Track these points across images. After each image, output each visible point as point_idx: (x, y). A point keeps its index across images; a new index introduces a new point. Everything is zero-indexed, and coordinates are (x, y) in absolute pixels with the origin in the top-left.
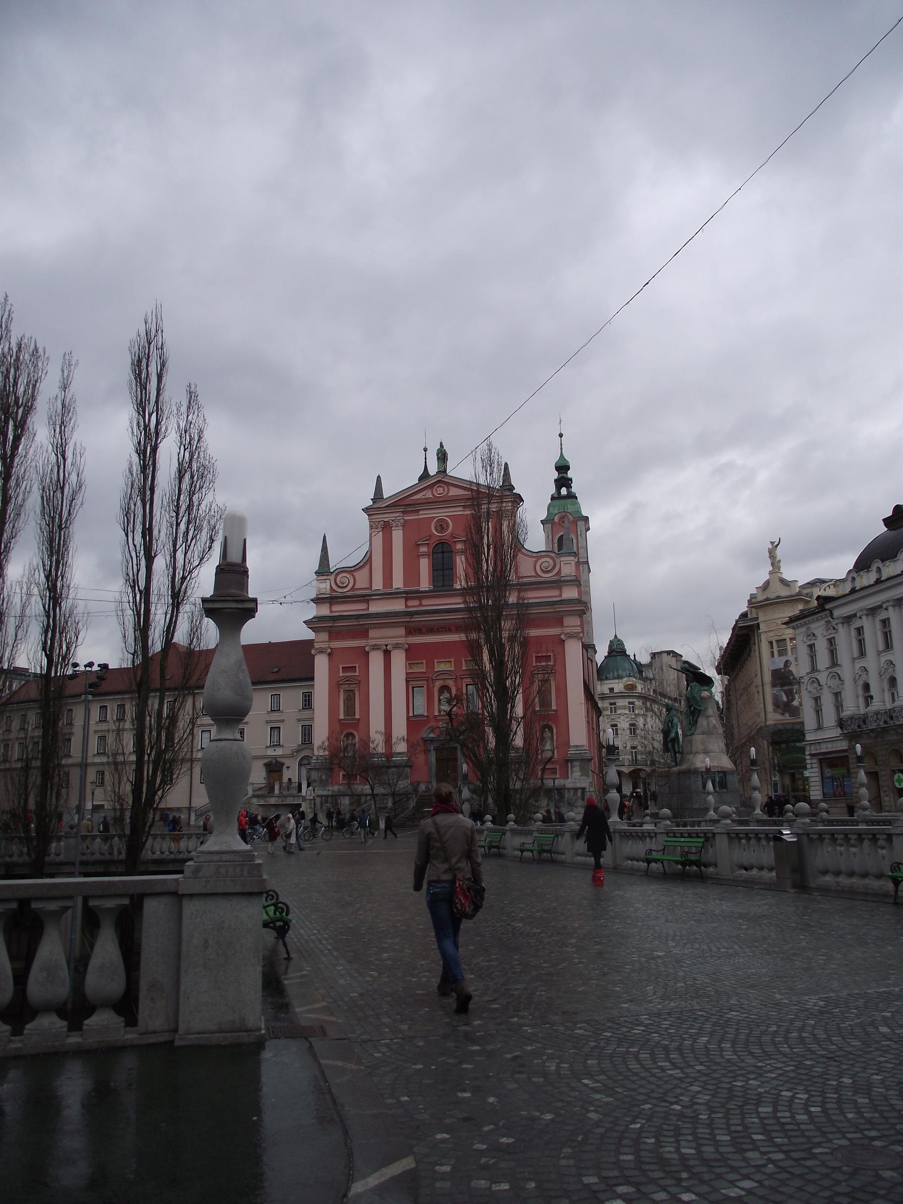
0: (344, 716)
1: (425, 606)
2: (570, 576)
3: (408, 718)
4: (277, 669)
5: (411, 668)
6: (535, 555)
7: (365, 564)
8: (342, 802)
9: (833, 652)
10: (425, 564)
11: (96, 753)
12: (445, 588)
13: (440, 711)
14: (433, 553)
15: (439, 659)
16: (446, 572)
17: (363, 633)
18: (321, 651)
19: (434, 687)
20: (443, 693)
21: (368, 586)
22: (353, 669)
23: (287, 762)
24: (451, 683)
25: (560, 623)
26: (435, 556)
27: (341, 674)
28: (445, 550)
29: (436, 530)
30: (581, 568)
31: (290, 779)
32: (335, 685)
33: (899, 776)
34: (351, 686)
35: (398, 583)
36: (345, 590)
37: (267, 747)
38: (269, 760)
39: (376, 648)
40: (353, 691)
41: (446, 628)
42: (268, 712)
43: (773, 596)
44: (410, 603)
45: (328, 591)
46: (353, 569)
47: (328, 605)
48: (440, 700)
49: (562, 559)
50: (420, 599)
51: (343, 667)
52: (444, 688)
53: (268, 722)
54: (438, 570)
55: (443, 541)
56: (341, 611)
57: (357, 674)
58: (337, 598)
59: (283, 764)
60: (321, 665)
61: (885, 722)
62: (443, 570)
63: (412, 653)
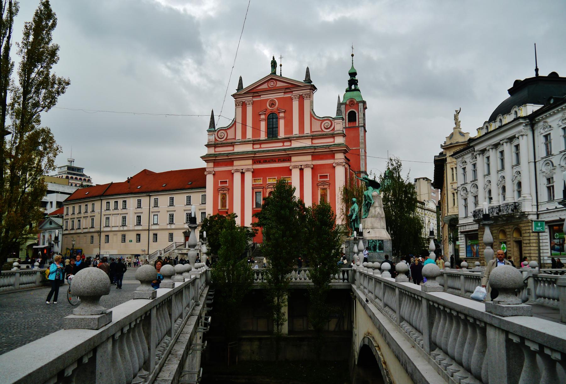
2: (339, 130)
3: (253, 208)
4: (191, 183)
5: (255, 182)
7: (233, 125)
9: (475, 171)
10: (263, 125)
11: (121, 225)
12: (273, 139)
14: (268, 119)
15: (270, 177)
16: (274, 129)
17: (230, 162)
18: (210, 173)
21: (234, 138)
22: (226, 182)
25: (333, 157)
26: (269, 120)
27: (220, 185)
28: (274, 117)
29: (270, 106)
30: (360, 130)
32: (217, 190)
33: (504, 246)
34: (225, 191)
35: (249, 135)
36: (222, 140)
37: (184, 224)
38: (186, 230)
39: (237, 171)
40: (225, 194)
41: (273, 160)
42: (185, 205)
43: (455, 142)
44: (255, 146)
45: (214, 141)
46: (226, 128)
47: (213, 148)
49: (336, 121)
50: (260, 144)
53: (185, 210)
54: (270, 128)
55: (273, 112)
57: (228, 185)
58: (218, 144)
60: (210, 179)
61: (497, 213)
62: (273, 128)
63: (256, 173)
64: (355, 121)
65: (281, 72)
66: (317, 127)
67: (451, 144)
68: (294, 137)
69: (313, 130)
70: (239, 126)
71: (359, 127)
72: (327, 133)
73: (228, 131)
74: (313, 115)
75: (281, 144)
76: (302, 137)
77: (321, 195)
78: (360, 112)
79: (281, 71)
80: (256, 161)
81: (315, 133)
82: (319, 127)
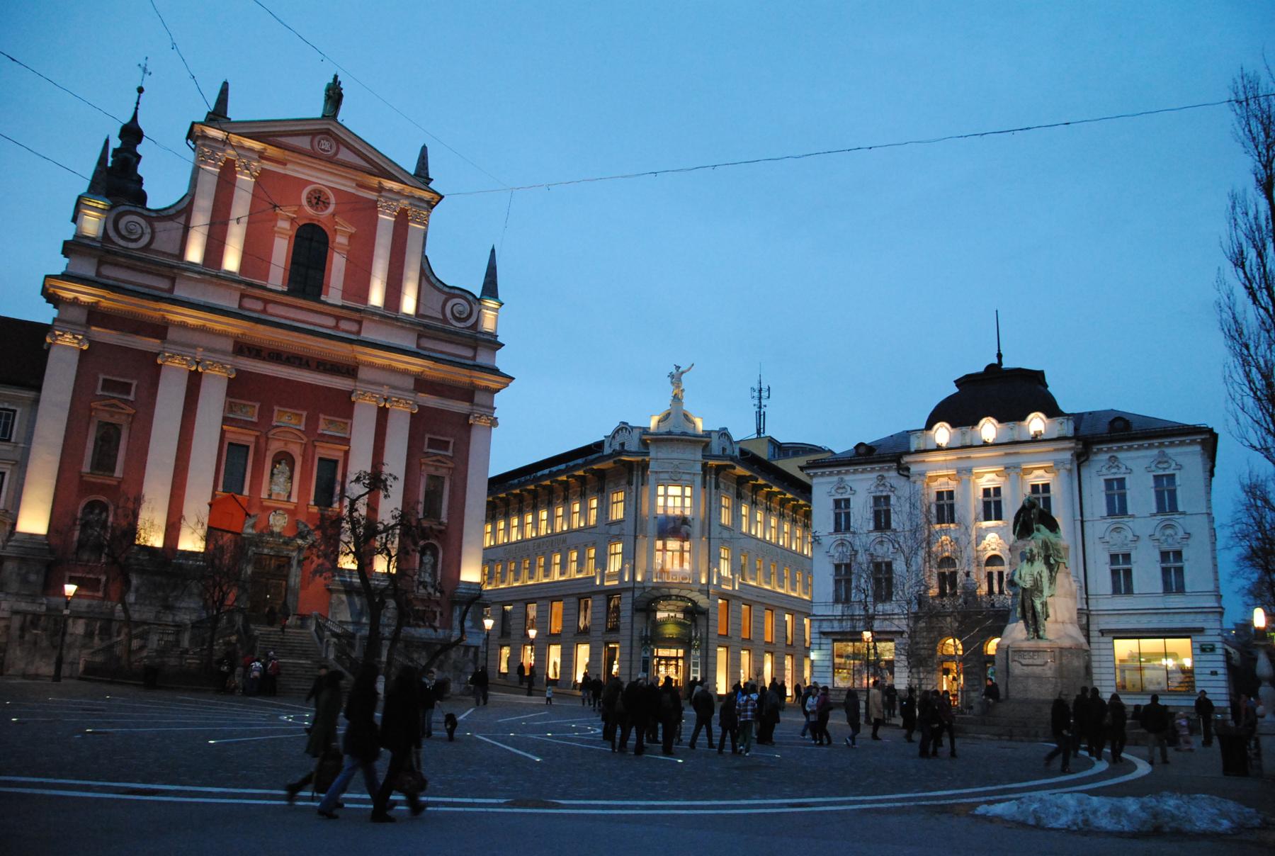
0: (91, 468)
1: (272, 315)
5: (231, 411)
6: (446, 290)
7: (179, 213)
8: (70, 630)
13: (270, 495)
14: (297, 236)
19: (266, 450)
20: (280, 463)
21: (177, 252)
24: (296, 450)
27: (99, 392)
29: (309, 202)
35: (231, 262)
40: (116, 428)
44: (248, 303)
46: (154, 215)
47: (95, 261)
48: (272, 474)
51: (105, 380)
56: (124, 281)
57: (131, 398)
63: (239, 387)
65: (137, 108)
67: (669, 433)
68: (374, 314)
69: (421, 311)
70: (200, 220)
72: (458, 330)
73: (156, 224)
74: (427, 272)
75: (331, 322)
76: (397, 319)
79: (138, 103)
81: (426, 321)
82: (440, 310)
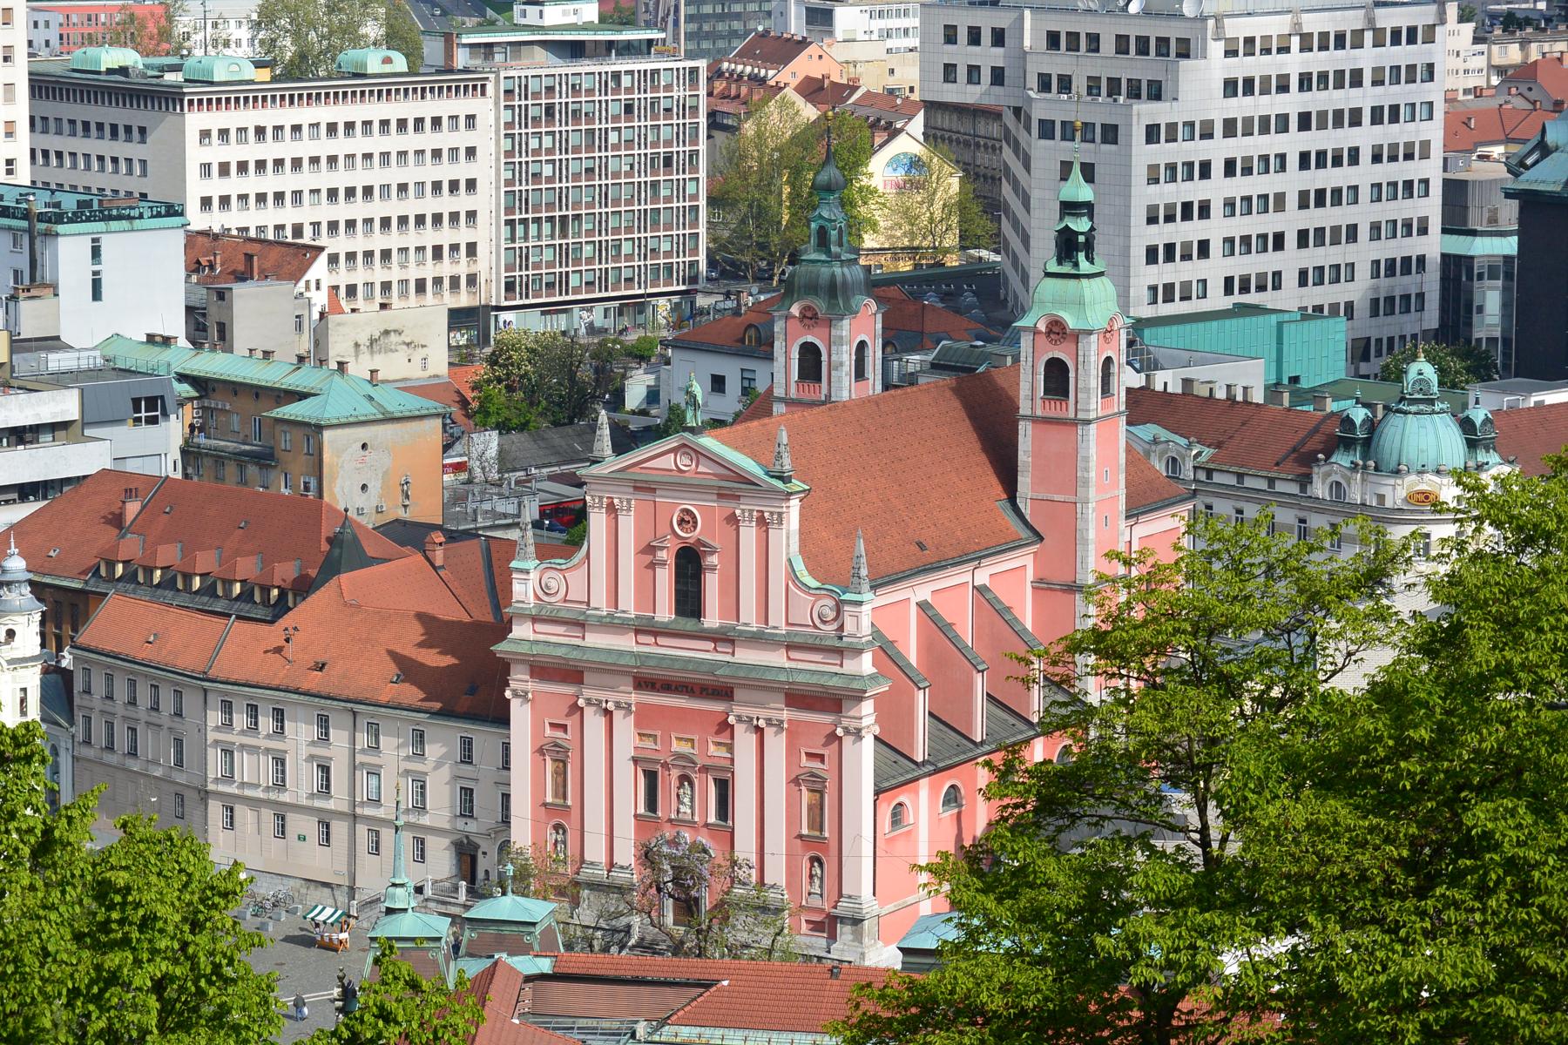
3: (636, 816)
13: (678, 812)
18: (523, 696)
23: (484, 845)
29: (679, 525)
30: (1080, 432)
31: (487, 872)
36: (553, 600)
44: (642, 638)
46: (564, 567)
48: (678, 796)
50: (655, 634)
52: (685, 779)
59: (477, 847)
60: (520, 714)
63: (645, 719)
64: (1066, 395)
66: (802, 615)
71: (1075, 423)
77: (810, 808)
78: (1080, 367)
80: (644, 683)
